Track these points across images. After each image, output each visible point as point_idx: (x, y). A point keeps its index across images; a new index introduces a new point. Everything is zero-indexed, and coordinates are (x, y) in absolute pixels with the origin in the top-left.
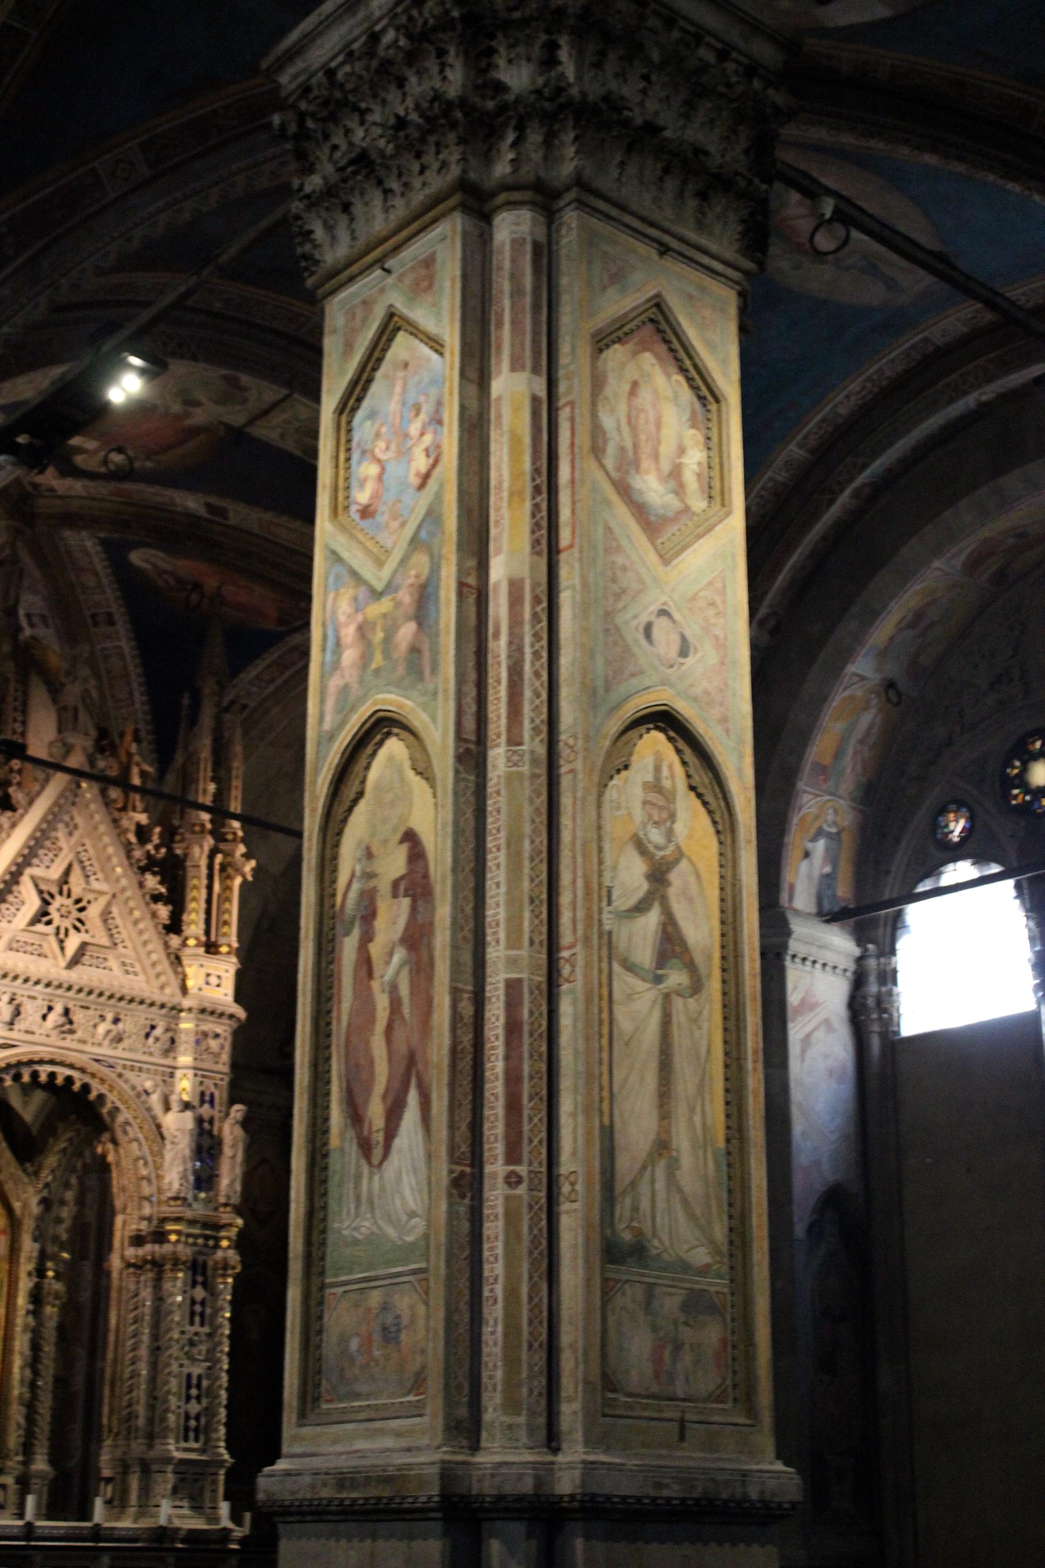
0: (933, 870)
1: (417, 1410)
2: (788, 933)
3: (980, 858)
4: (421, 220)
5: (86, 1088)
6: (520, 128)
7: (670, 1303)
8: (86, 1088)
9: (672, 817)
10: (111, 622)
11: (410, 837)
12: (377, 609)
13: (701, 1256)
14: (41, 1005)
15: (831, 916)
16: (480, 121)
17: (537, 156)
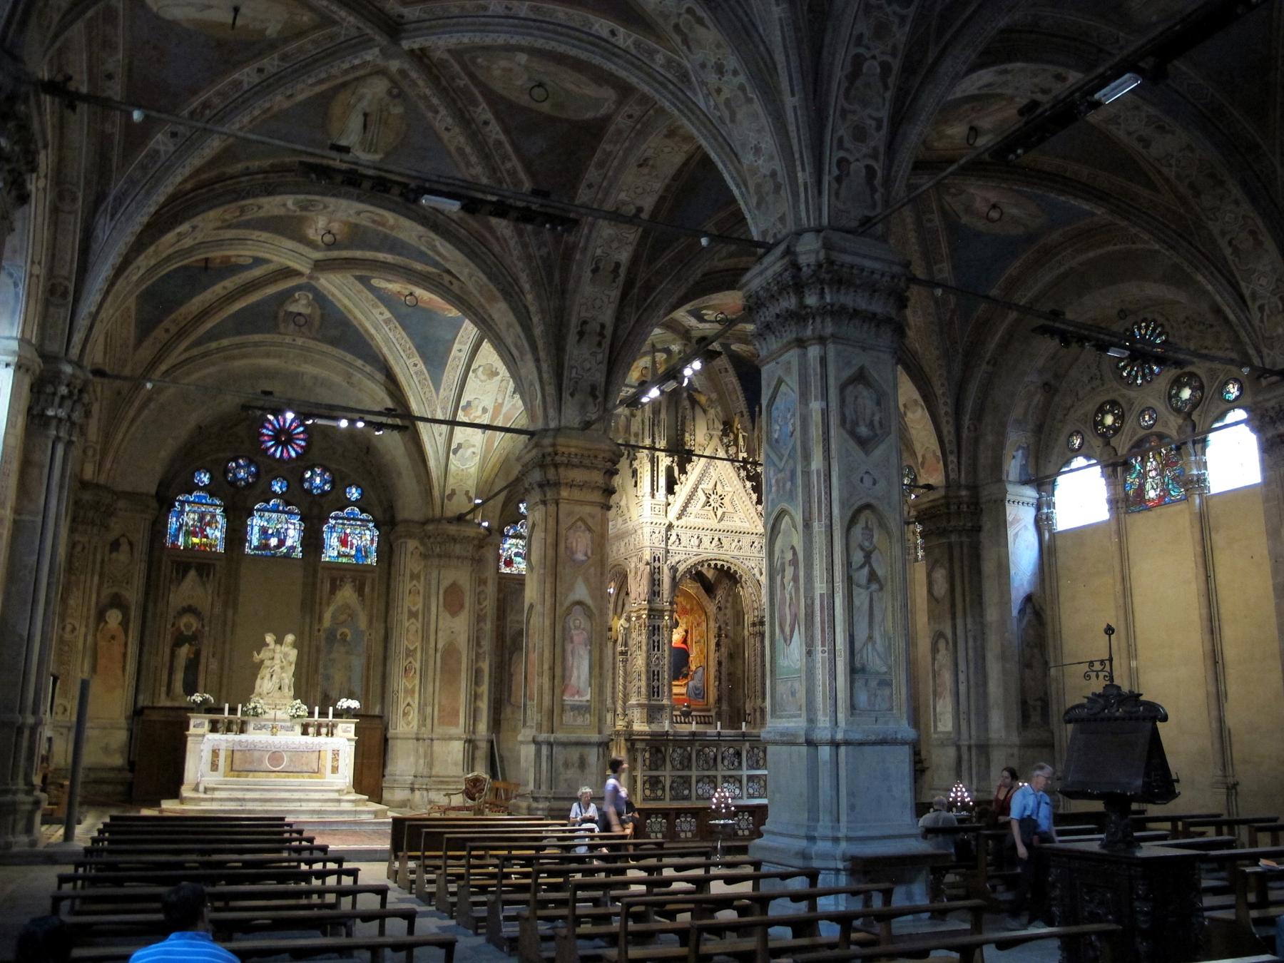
0: (1068, 462)
1: (800, 716)
2: (1006, 492)
3: (1088, 457)
4: (787, 347)
5: (729, 568)
6: (814, 318)
7: (873, 684)
8: (729, 568)
9: (872, 536)
10: (726, 370)
11: (793, 548)
12: (780, 476)
13: (884, 669)
14: (710, 538)
15: (1024, 483)
16: (799, 316)
17: (819, 327)
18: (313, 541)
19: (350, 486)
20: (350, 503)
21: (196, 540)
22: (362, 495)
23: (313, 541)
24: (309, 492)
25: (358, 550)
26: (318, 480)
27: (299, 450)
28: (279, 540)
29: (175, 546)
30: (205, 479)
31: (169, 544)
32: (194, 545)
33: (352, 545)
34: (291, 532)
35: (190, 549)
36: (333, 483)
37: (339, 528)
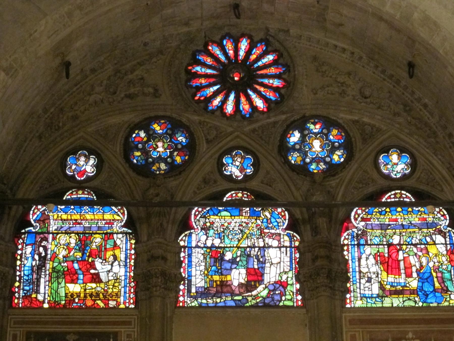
18: (323, 269)
19: (386, 150)
20: (392, 184)
21: (75, 288)
22: (413, 165)
23: (323, 269)
24: (302, 169)
25: (425, 278)
26: (317, 144)
27: (271, 95)
28: (250, 272)
29: (33, 305)
30: (87, 166)
31: (18, 301)
32: (70, 298)
33: (408, 268)
34: (273, 254)
35: (62, 309)
36: (348, 146)
37: (375, 236)
